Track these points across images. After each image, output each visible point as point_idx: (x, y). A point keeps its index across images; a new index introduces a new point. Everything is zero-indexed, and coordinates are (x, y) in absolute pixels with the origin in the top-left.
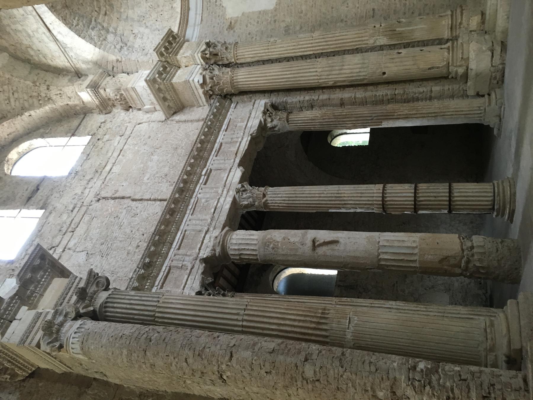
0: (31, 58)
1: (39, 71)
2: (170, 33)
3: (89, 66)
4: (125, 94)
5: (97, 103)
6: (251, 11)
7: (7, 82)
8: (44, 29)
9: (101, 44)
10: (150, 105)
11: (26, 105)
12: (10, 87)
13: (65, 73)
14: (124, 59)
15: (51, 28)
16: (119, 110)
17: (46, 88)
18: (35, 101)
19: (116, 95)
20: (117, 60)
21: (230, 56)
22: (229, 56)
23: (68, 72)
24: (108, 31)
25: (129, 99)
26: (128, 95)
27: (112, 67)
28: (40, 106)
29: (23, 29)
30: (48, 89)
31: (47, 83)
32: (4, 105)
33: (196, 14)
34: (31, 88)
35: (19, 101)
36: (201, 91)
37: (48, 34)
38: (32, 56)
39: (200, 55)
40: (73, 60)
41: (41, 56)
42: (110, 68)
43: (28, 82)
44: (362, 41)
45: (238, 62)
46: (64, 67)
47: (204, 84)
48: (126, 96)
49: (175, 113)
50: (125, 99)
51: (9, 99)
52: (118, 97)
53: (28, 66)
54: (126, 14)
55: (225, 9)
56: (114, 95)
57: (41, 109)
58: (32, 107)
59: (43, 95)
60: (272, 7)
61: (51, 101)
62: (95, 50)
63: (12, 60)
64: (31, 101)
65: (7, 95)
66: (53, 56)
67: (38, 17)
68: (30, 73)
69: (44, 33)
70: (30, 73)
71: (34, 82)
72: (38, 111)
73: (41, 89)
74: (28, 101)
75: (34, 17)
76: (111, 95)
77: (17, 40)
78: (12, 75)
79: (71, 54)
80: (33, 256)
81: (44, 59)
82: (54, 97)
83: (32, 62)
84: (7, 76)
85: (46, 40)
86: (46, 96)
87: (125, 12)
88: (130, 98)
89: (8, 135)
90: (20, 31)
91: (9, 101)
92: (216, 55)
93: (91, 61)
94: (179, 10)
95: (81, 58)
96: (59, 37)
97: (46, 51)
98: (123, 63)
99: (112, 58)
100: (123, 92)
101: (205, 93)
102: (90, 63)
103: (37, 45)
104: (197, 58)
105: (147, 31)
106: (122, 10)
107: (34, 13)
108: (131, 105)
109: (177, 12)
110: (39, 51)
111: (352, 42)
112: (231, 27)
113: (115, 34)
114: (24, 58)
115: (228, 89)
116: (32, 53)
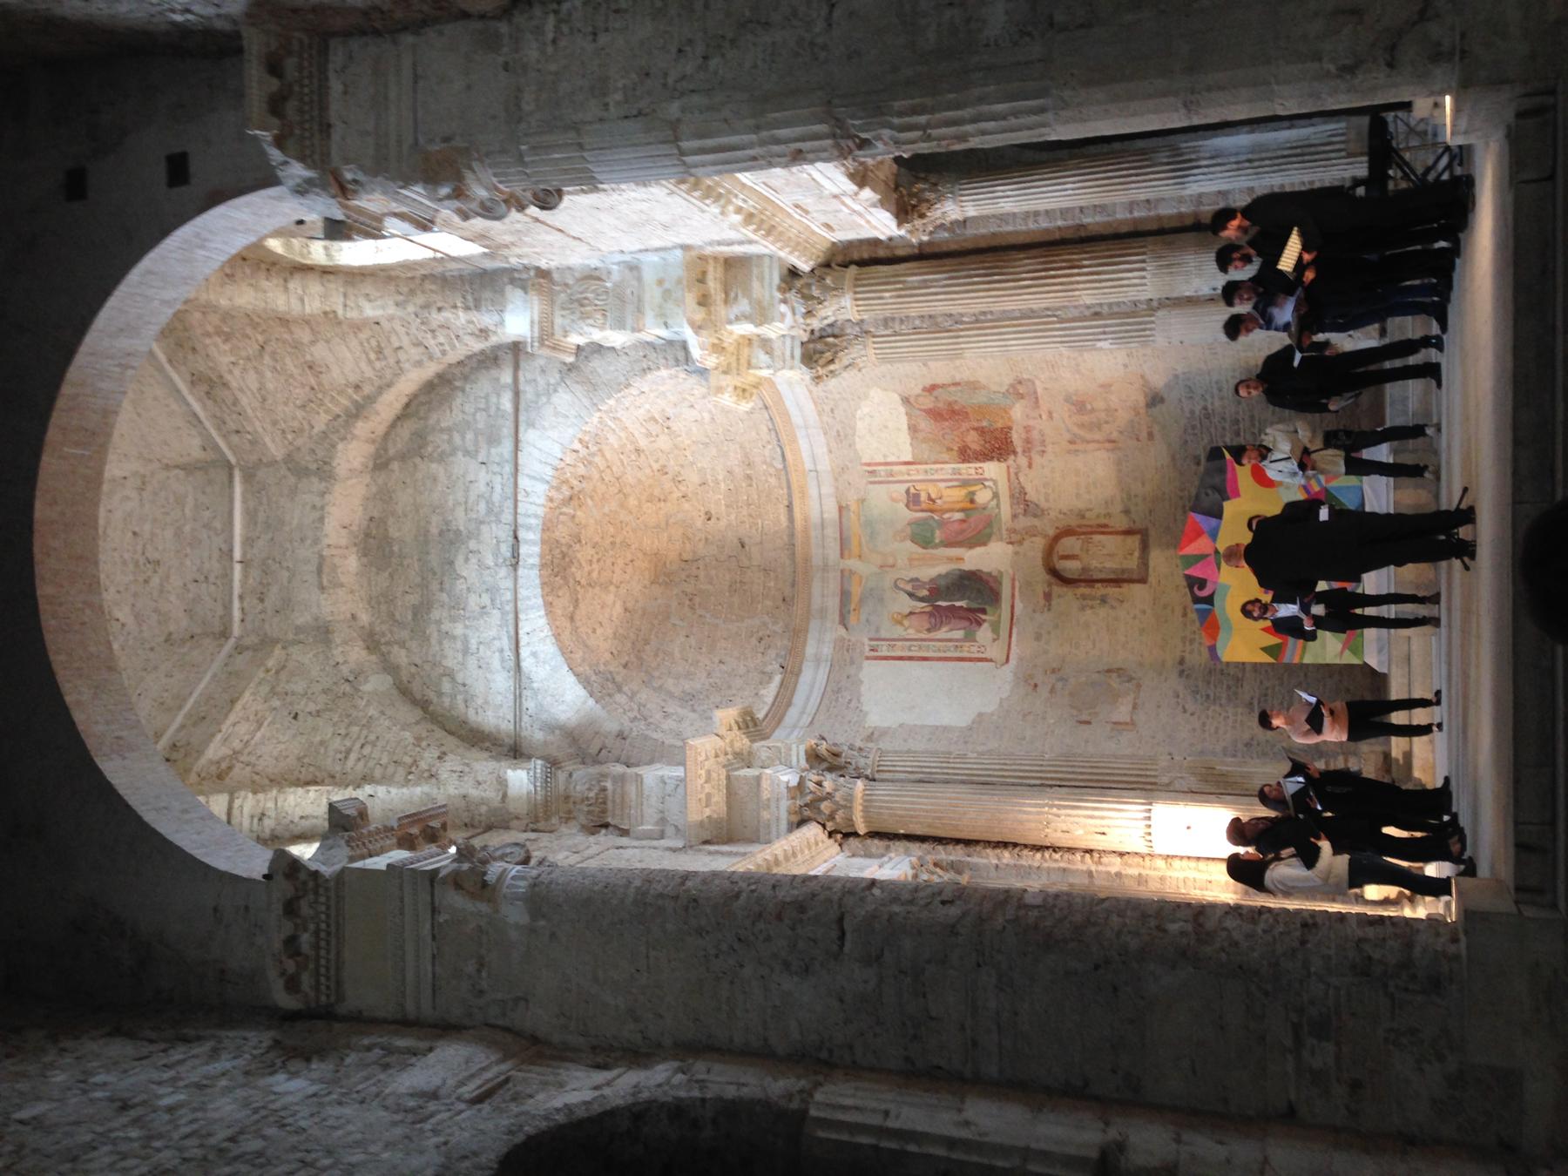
0: (435, 700)
1: (435, 728)
3: (550, 738)
4: (610, 792)
5: (539, 798)
6: (918, 723)
7: (364, 721)
8: (506, 643)
9: (602, 698)
10: (657, 823)
11: (378, 773)
12: (365, 732)
13: (487, 744)
14: (634, 734)
15: (522, 643)
16: (574, 831)
17: (437, 754)
18: (401, 771)
19: (589, 789)
21: (866, 763)
22: (862, 762)
23: (494, 745)
24: (619, 689)
25: (614, 801)
26: (619, 790)
27: (598, 748)
28: (407, 782)
29: (465, 636)
30: (439, 758)
31: (444, 749)
32: (329, 761)
33: (803, 713)
34: (406, 747)
35: (367, 762)
37: (509, 654)
38: (440, 694)
39: (802, 748)
40: (526, 718)
41: (459, 697)
42: (593, 750)
43: (407, 734)
44: (1147, 776)
45: (877, 776)
46: (494, 731)
48: (610, 798)
49: (706, 842)
50: (605, 803)
51: (348, 752)
52: (592, 794)
53: (419, 713)
54: (660, 683)
55: (866, 714)
56: (587, 786)
57: (405, 790)
58: (386, 780)
59: (423, 765)
60: (964, 725)
61: (434, 780)
62: (585, 703)
63: (395, 692)
64: (391, 769)
65: (348, 743)
66: (486, 702)
67: (511, 617)
68: (417, 723)
69: (501, 651)
70: (417, 723)
71: (419, 739)
72: (394, 791)
73: (426, 755)
74: (386, 768)
75: (504, 614)
76: (578, 788)
77: (434, 656)
78: (383, 713)
79: (529, 704)
80: (432, 813)
81: (461, 706)
82: (444, 775)
83: (431, 708)
84: (372, 712)
85: (496, 663)
86: (429, 770)
87: (659, 678)
88: (618, 801)
89: (302, 817)
90: (454, 638)
91: (346, 758)
93: (561, 728)
94: (770, 700)
95: (544, 716)
96: (527, 663)
97: (478, 688)
98: (628, 741)
99: (611, 726)
100: (609, 785)
102: (557, 732)
103: (471, 674)
104: (794, 752)
105: (692, 715)
106: (656, 674)
107: (509, 608)
108: (609, 820)
109: (764, 703)
110: (464, 685)
111: (1125, 775)
112: (870, 738)
113: (631, 699)
114: (418, 697)
116: (446, 686)
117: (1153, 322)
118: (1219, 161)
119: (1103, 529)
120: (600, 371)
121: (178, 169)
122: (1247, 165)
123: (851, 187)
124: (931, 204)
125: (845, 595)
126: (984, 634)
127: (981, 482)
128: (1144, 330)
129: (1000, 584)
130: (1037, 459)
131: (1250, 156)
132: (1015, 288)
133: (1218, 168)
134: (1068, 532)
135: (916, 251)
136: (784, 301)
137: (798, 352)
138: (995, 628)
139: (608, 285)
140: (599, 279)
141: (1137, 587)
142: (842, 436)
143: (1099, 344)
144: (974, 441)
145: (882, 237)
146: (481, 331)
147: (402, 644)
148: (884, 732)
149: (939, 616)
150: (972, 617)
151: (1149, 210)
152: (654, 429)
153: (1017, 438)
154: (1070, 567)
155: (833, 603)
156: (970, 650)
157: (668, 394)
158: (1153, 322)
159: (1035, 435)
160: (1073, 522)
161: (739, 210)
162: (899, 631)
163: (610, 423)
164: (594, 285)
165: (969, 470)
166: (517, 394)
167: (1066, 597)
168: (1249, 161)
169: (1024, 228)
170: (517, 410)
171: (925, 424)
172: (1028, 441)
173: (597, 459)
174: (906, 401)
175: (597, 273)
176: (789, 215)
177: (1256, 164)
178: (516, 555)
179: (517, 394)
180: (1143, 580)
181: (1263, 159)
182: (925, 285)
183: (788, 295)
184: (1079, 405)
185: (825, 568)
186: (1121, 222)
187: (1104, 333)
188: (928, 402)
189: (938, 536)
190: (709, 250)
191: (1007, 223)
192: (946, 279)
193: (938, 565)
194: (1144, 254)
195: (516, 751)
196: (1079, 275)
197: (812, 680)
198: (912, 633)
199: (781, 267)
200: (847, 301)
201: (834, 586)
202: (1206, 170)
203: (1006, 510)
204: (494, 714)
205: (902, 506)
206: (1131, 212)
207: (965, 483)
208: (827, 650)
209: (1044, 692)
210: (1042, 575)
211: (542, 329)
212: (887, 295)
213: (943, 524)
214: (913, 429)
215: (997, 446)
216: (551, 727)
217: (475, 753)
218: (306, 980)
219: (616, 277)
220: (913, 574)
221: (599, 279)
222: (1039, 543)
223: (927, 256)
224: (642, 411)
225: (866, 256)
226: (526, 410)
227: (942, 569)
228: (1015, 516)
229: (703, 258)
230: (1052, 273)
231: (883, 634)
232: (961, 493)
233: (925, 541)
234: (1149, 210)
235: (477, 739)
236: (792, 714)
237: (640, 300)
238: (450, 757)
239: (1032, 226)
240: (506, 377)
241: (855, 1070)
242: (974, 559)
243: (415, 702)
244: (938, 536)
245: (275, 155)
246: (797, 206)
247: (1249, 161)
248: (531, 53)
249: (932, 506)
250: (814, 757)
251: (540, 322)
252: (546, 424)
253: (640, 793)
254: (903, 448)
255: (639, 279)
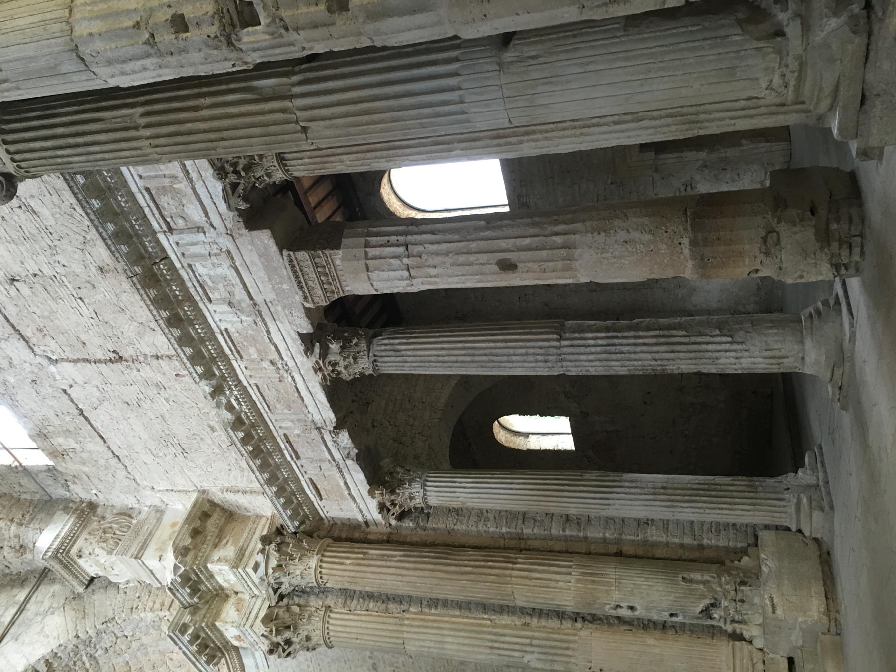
117: (575, 642)
118: (638, 484)
120: (97, 603)
122: (662, 491)
123: (329, 416)
124: (401, 483)
128: (568, 648)
131: (664, 485)
132: (457, 573)
133: (638, 490)
135: (385, 538)
136: (262, 551)
137: (262, 614)
139: (134, 522)
140: (130, 516)
143: (527, 657)
145: (361, 519)
146: (21, 546)
151: (580, 531)
157: (150, 650)
158: (575, 642)
161: (230, 408)
163: (84, 658)
164: (123, 520)
166: (21, 610)
168: (663, 488)
169: (474, 528)
170: (12, 623)
175: (130, 512)
176: (281, 451)
177: (670, 491)
179: (21, 610)
181: (676, 489)
182: (381, 558)
183: (267, 547)
186: (558, 539)
187: (531, 645)
190: (218, 496)
191: (462, 523)
192: (401, 556)
194: (572, 561)
196: (513, 569)
199: (271, 524)
200: (313, 562)
202: (627, 490)
206: (564, 530)
211: (62, 543)
212: (348, 562)
219: (142, 516)
221: (130, 516)
223: (391, 540)
224: (120, 659)
225: (344, 535)
226: (19, 626)
229: (213, 504)
230: (490, 564)
234: (580, 531)
237: (151, 535)
239: (482, 528)
240: (22, 595)
246: (288, 441)
247: (663, 488)
251: (65, 538)
252: (27, 640)
255: (159, 520)
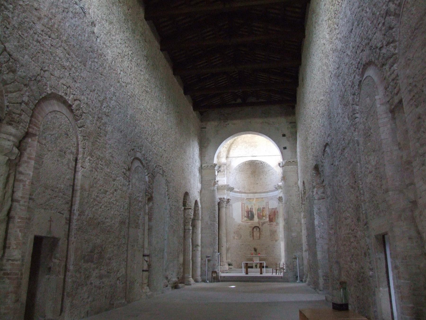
2: (234, 189)
20: (230, 172)
36: (222, 197)
38: (234, 145)
39: (229, 198)
41: (234, 148)
42: (228, 168)
47: (224, 198)
79: (234, 159)
82: (223, 149)
92: (229, 202)
100: (223, 173)
101: (221, 198)
107: (246, 156)
115: (221, 205)
116: (235, 146)
119: (260, 234)
121: (285, 148)
125: (250, 199)
126: (246, 219)
127: (266, 218)
129: (253, 220)
130: (269, 225)
134: (260, 229)
137: (281, 196)
138: (246, 220)
141: (252, 239)
142: (272, 198)
144: (271, 217)
147: (241, 139)
148: (232, 207)
149: (248, 212)
150: (248, 217)
152: (272, 173)
153: (271, 223)
154: (255, 230)
155: (249, 197)
156: (243, 217)
159: (272, 225)
160: (261, 230)
162: (246, 207)
165: (268, 216)
167: (251, 229)
171: (273, 210)
172: (271, 224)
173: (267, 166)
174: (276, 208)
178: (254, 156)
180: (253, 239)
184: (275, 231)
185: (254, 196)
188: (276, 211)
189: (259, 212)
193: (255, 212)
195: (227, 157)
197: (239, 195)
198: (245, 209)
201: (252, 197)
203: (262, 221)
204: (232, 154)
205: (263, 207)
207: (266, 215)
208: (243, 197)
209: (238, 227)
210: (254, 226)
213: (261, 212)
214: (273, 209)
215: (271, 220)
216: (230, 162)
217: (227, 151)
218: (205, 167)
220: (254, 209)
222: (258, 226)
227: (254, 212)
228: (261, 222)
231: (245, 205)
232: (264, 214)
233: (258, 210)
235: (229, 151)
236: (234, 193)
238: (226, 149)
241: (202, 223)
242: (256, 217)
243: (233, 142)
244: (259, 212)
245: (285, 161)
248: (294, 188)
249: (263, 211)
250: (228, 200)
253: (222, 177)
254: (270, 207)
